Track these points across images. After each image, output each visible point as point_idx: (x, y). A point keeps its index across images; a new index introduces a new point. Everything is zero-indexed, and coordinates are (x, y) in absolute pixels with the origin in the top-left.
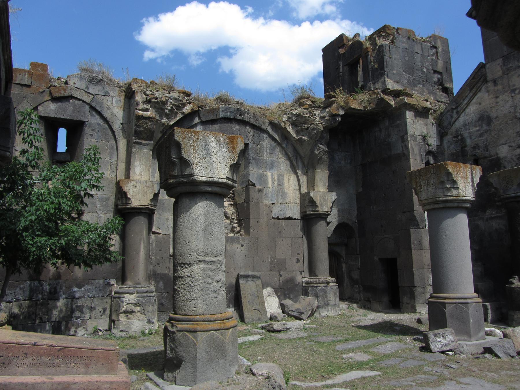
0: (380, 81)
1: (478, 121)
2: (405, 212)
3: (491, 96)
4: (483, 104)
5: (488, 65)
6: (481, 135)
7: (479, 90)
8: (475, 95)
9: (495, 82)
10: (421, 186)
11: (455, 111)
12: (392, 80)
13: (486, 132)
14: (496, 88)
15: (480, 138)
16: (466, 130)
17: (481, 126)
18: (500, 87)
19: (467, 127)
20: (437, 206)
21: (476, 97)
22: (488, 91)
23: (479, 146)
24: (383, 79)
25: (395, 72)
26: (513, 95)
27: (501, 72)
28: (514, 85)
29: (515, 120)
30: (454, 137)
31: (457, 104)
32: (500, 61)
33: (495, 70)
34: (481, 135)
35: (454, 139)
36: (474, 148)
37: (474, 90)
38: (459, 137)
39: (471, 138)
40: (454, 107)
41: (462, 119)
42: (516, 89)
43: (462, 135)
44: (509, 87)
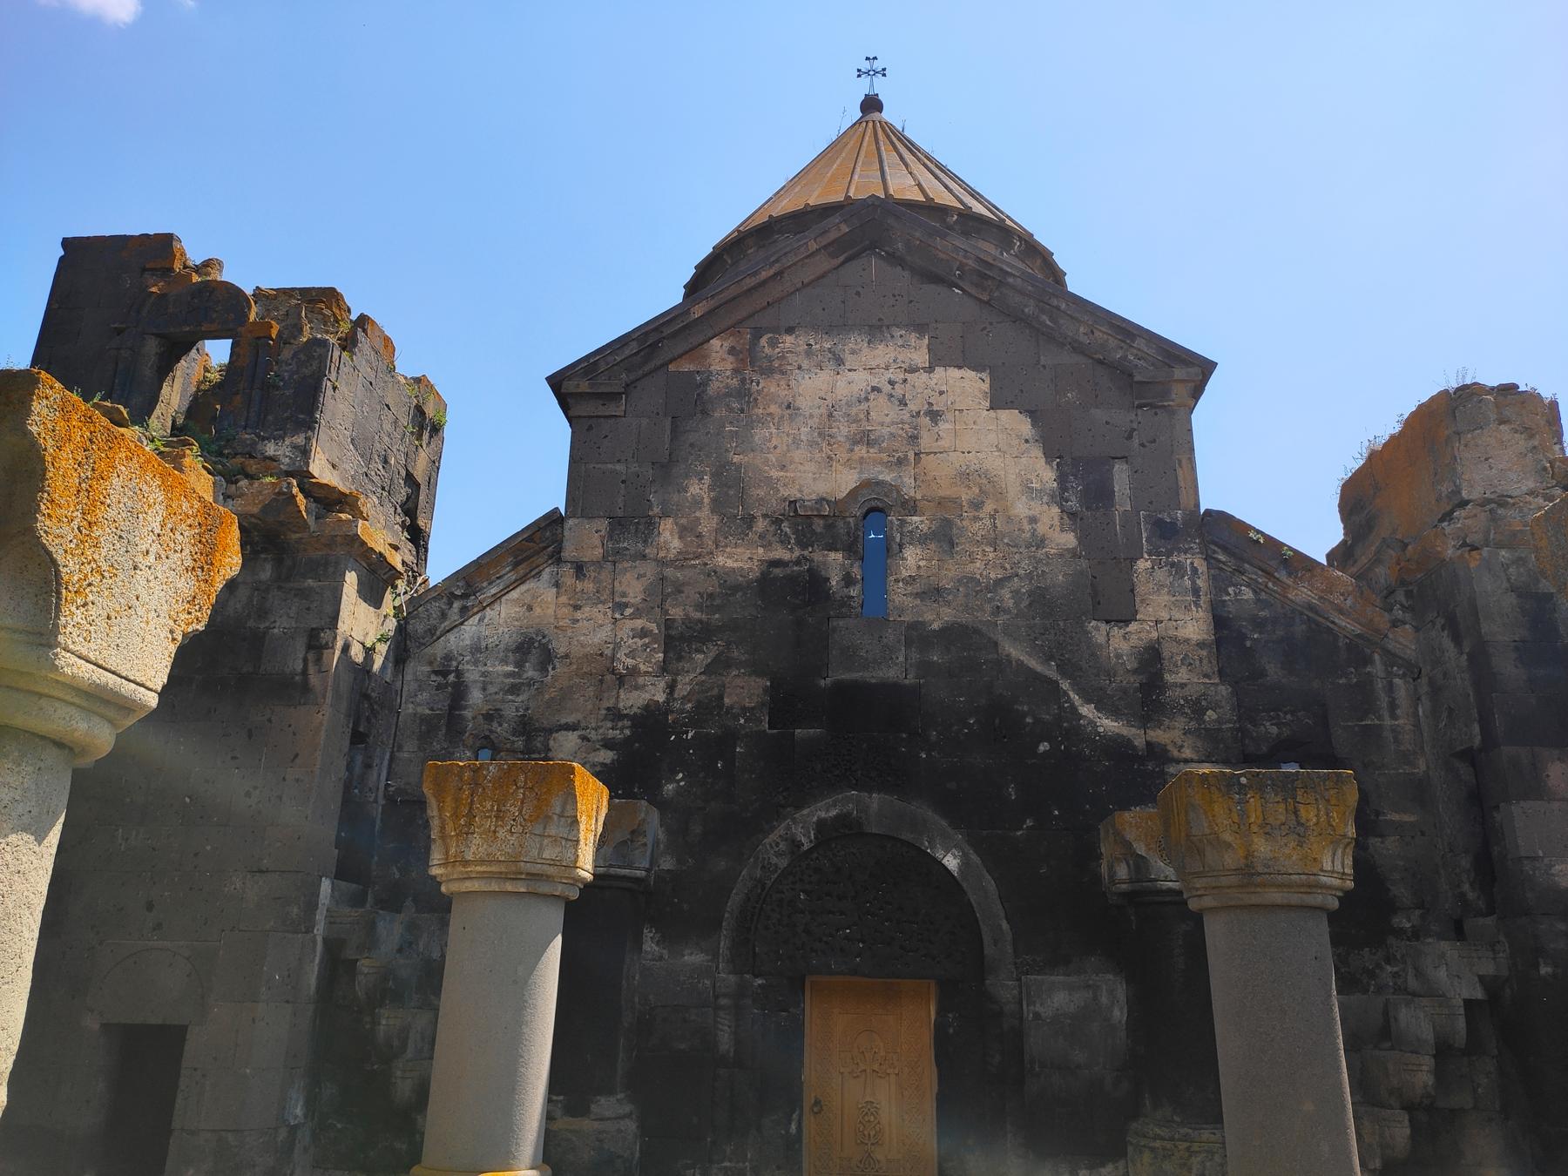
2: (261, 871)
3: (563, 599)
4: (537, 611)
5: (571, 522)
6: (514, 689)
7: (533, 574)
8: (521, 581)
9: (580, 569)
10: (471, 816)
11: (457, 605)
13: (529, 685)
14: (579, 586)
16: (476, 663)
17: (520, 664)
18: (589, 586)
19: (481, 657)
20: (509, 887)
21: (523, 588)
22: (557, 585)
24: (300, 439)
26: (617, 616)
27: (598, 552)
28: (624, 595)
29: (609, 677)
30: (436, 673)
31: (468, 585)
32: (603, 524)
33: (586, 539)
34: (514, 689)
35: (433, 677)
36: (489, 717)
37: (522, 570)
38: (451, 678)
39: (484, 689)
40: (458, 593)
41: (470, 629)
42: (626, 605)
43: (459, 673)
44: (613, 593)
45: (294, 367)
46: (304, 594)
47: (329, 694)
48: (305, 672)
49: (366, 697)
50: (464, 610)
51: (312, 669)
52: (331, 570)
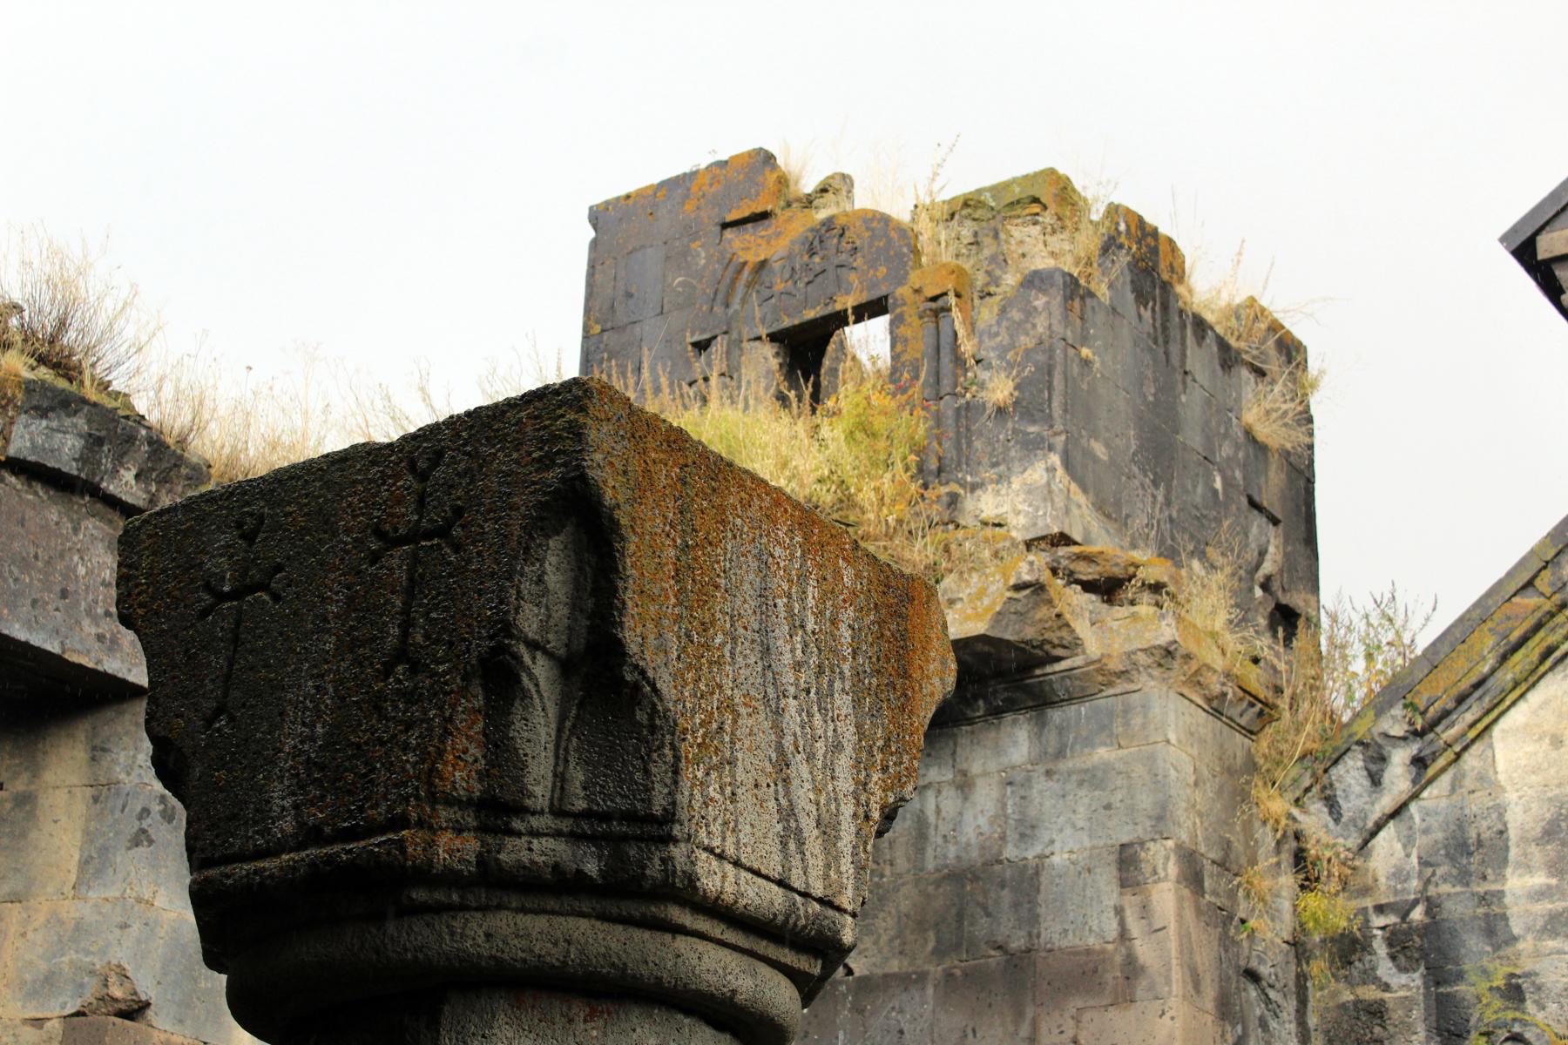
0: (1016, 483)
1: (1539, 841)
12: (1085, 490)
15: (1551, 944)
21: (1534, 697)
23: (1539, 988)
25: (1099, 450)
38: (1417, 914)
45: (1003, 338)
46: (1093, 779)
47: (1177, 974)
48: (1124, 935)
49: (1253, 976)
50: (1419, 762)
51: (1135, 927)
52: (1137, 721)
